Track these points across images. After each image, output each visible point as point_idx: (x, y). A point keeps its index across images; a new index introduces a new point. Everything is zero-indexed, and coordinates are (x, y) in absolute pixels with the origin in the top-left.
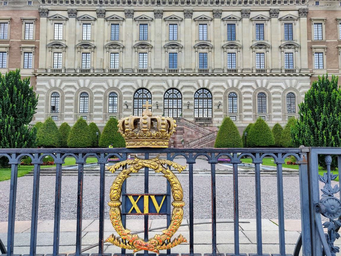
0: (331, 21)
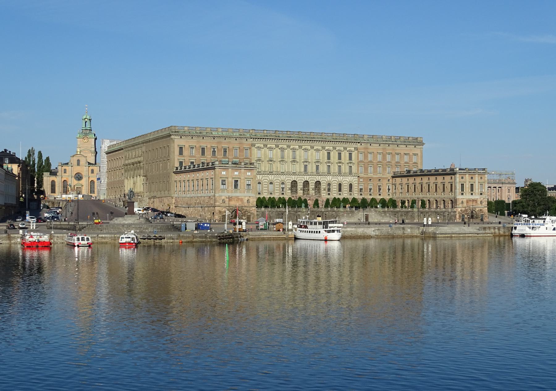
0: (366, 153)
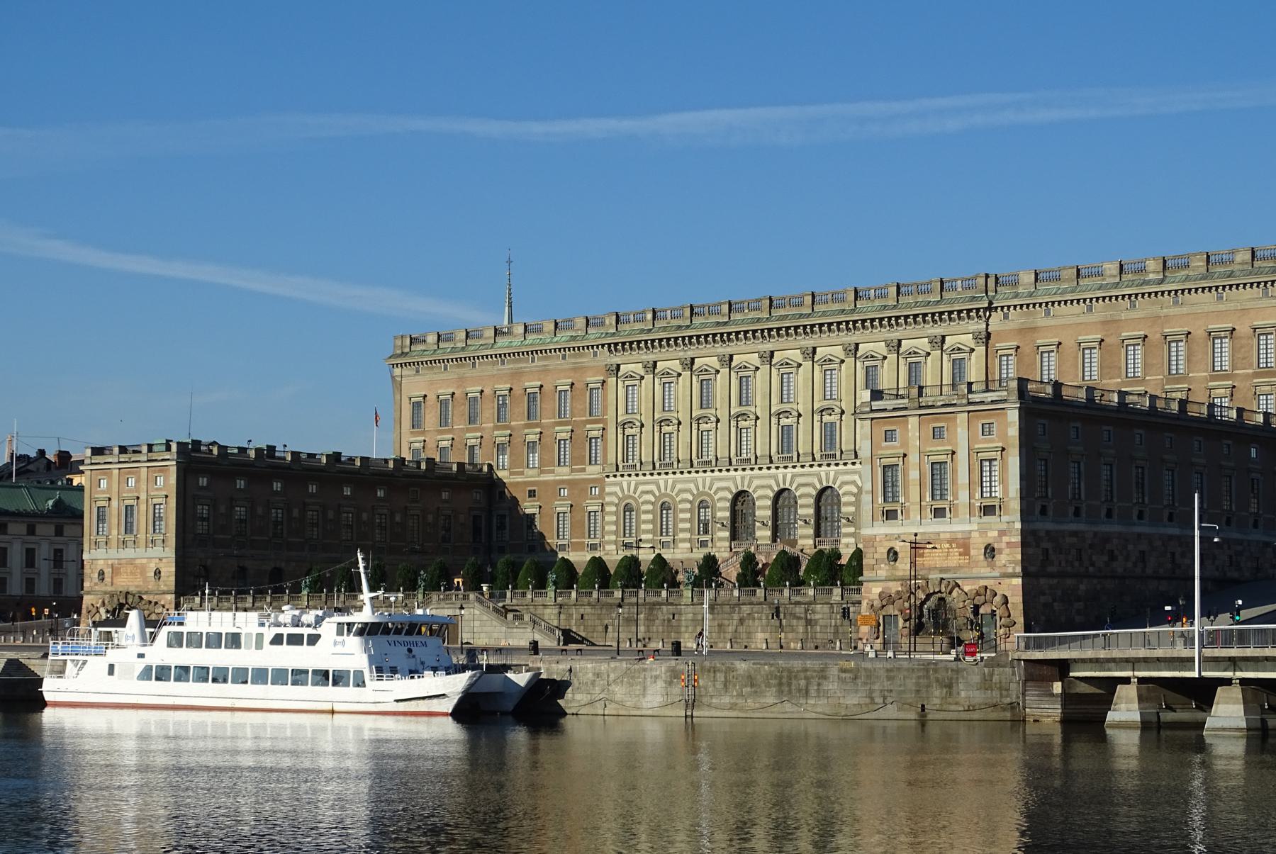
0: (1027, 349)
